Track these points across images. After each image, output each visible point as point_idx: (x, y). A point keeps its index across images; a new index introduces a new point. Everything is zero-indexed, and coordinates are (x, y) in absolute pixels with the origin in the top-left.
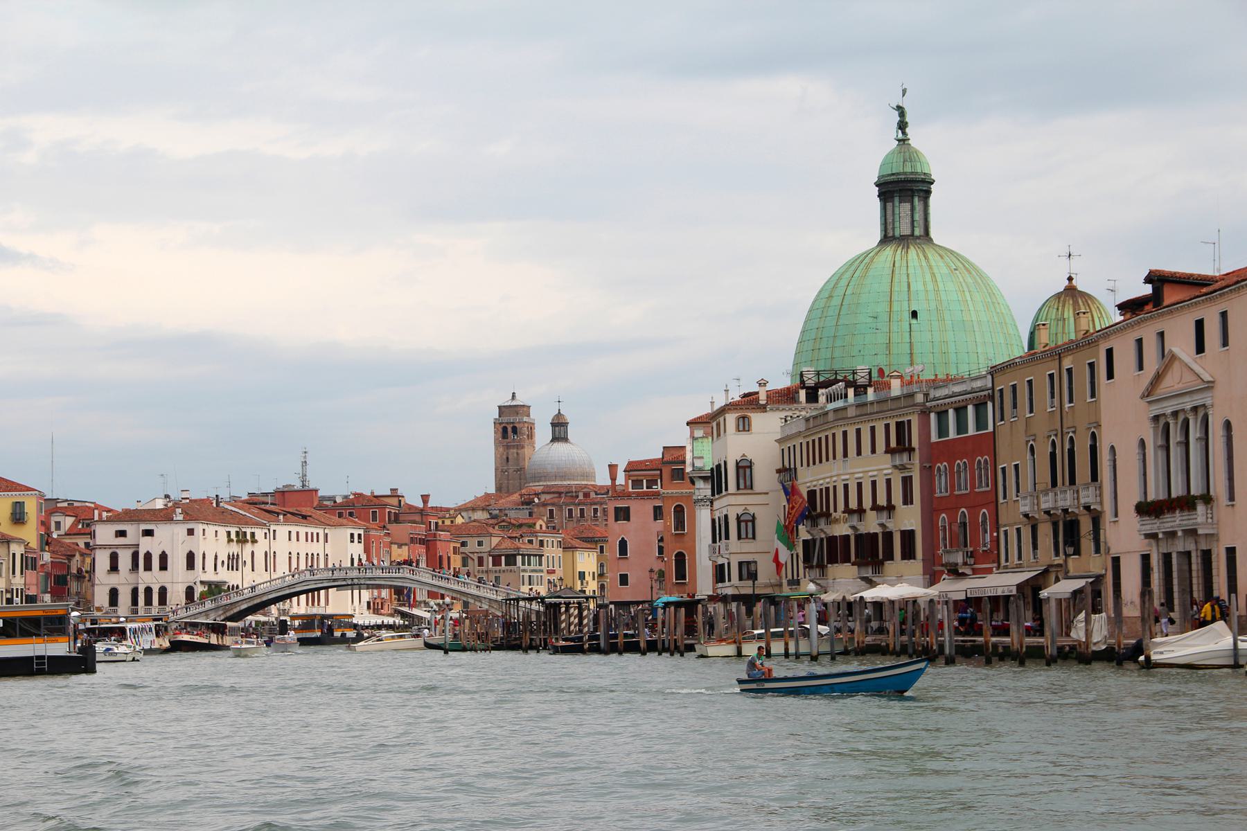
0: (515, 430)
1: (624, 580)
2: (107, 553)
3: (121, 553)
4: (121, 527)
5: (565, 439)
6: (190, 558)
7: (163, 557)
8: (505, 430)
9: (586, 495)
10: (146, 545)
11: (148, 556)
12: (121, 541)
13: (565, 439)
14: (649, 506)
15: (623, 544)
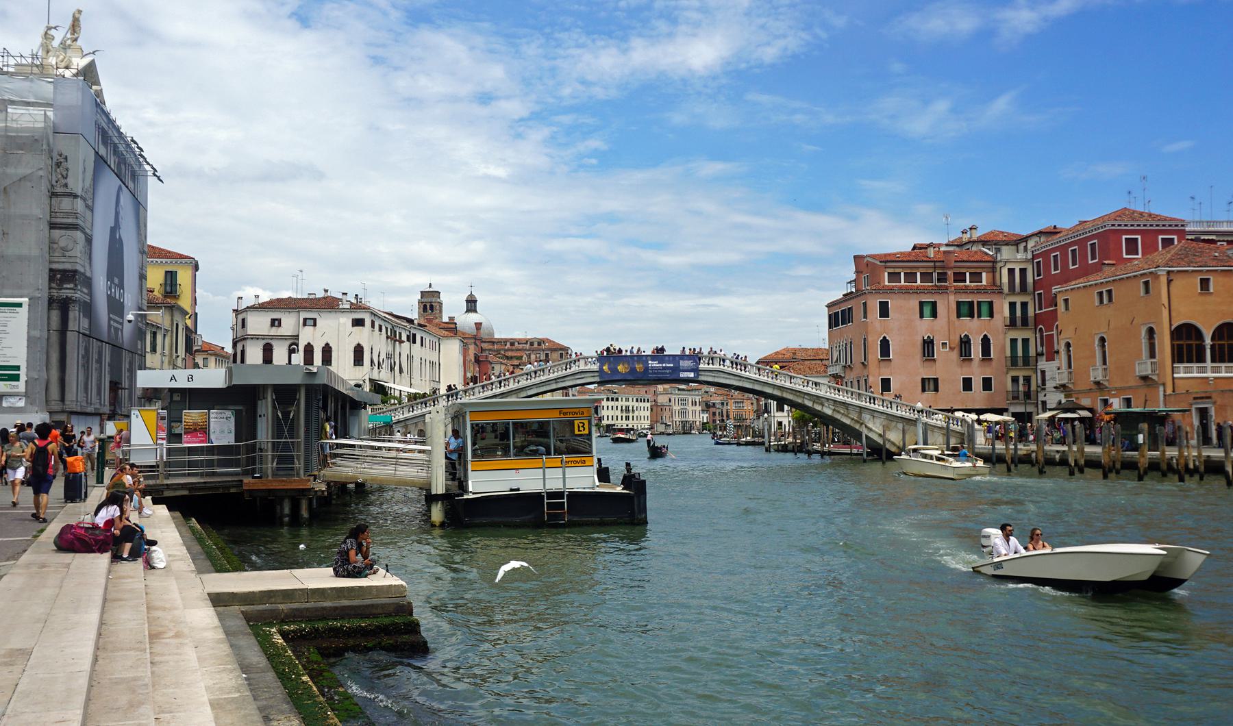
0: (432, 308)
1: (886, 385)
2: (261, 343)
3: (273, 343)
4: (275, 316)
5: (475, 311)
6: (359, 352)
7: (327, 350)
8: (425, 307)
9: (512, 344)
10: (307, 335)
11: (309, 350)
12: (274, 331)
13: (475, 311)
14: (914, 303)
15: (885, 344)
